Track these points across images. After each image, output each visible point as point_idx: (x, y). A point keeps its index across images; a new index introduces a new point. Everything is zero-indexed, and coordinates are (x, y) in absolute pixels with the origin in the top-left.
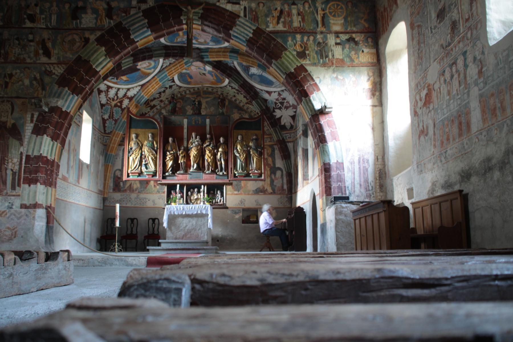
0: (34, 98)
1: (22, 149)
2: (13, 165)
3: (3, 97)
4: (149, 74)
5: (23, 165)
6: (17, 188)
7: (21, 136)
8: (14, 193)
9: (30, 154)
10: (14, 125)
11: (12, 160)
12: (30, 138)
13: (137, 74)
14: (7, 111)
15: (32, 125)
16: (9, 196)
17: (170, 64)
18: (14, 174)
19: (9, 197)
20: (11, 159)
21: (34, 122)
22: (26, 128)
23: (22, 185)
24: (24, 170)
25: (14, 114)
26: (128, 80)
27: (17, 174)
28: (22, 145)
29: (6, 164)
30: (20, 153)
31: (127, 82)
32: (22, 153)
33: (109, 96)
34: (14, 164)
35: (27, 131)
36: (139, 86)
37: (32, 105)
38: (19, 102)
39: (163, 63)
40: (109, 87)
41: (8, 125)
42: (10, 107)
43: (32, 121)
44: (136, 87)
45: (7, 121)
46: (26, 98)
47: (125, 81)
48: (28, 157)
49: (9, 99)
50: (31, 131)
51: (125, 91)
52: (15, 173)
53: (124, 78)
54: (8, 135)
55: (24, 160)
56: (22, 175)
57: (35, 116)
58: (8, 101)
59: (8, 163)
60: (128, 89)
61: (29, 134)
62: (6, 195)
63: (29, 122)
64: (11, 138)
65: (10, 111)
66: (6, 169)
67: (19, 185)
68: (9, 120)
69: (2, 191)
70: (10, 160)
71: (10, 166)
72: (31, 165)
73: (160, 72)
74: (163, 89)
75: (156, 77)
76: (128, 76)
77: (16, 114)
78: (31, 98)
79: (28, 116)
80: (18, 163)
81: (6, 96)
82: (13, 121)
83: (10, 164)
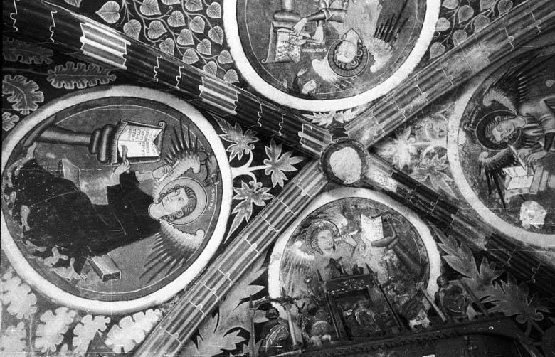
4: (185, 257)
13: (148, 246)
17: (257, 210)
26: (118, 274)
31: (115, 287)
33: (38, 343)
36: (154, 307)
39: (235, 203)
40: (46, 305)
44: (144, 311)
47: (107, 278)
51: (101, 323)
53: (101, 263)
60: (115, 319)
73: (222, 248)
74: (235, 338)
75: (209, 269)
76: (114, 254)
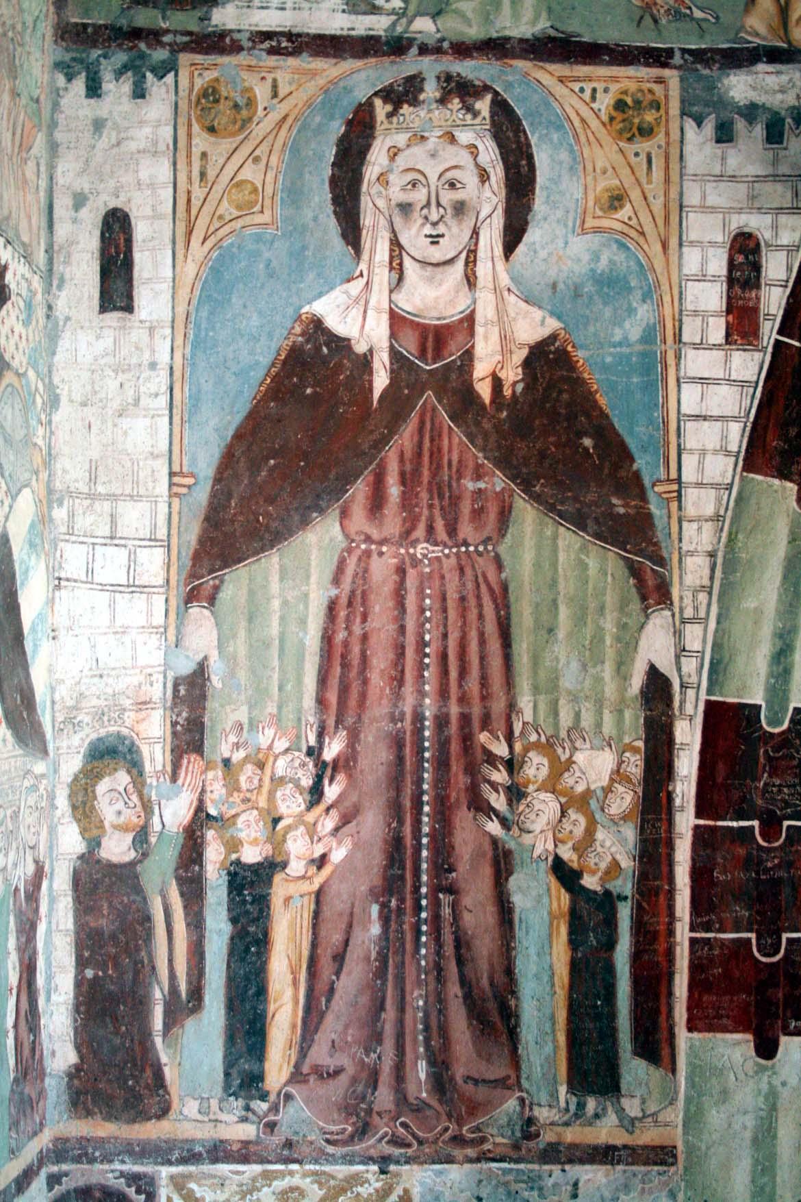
0: (741, 57)
1: (655, 644)
2: (577, 823)
3: (397, 46)
5: (686, 821)
6: (634, 1070)
7: (634, 487)
8: (607, 1131)
9: (756, 697)
10: (547, 360)
11: (560, 768)
12: (738, 518)
14: (460, 208)
15: (749, 365)
16: (554, 1154)
18: (589, 916)
19: (554, 1174)
20: (548, 748)
21: (769, 332)
22: (690, 399)
23: (683, 1037)
24: (699, 875)
25: (533, 235)
27: (625, 914)
28: (653, 590)
29: (498, 801)
30: (637, 680)
32: (657, 688)
34: (582, 801)
35: (699, 436)
37: (724, 134)
38: (567, 102)
41: (481, 369)
42: (489, 153)
43: (741, 323)
45: (469, 320)
46: (659, 58)
48: (726, 722)
49: (468, 69)
50: (736, 436)
52: (608, 901)
54: (498, 482)
55: (687, 765)
56: (683, 933)
57: (778, 269)
58: (460, 90)
59: (516, 793)
61: (722, 468)
62: (515, 1153)
63: (717, 333)
64: (526, 513)
65: (490, 203)
66: (502, 863)
67: (654, 1044)
68: (486, 310)
69: (474, 1108)
70: (536, 768)
71: (541, 826)
72: (771, 825)
77: (560, 241)
78: (699, 56)
79: (692, 260)
80: (624, 800)
81: (424, 26)
82: (532, 326)
83: (543, 809)
